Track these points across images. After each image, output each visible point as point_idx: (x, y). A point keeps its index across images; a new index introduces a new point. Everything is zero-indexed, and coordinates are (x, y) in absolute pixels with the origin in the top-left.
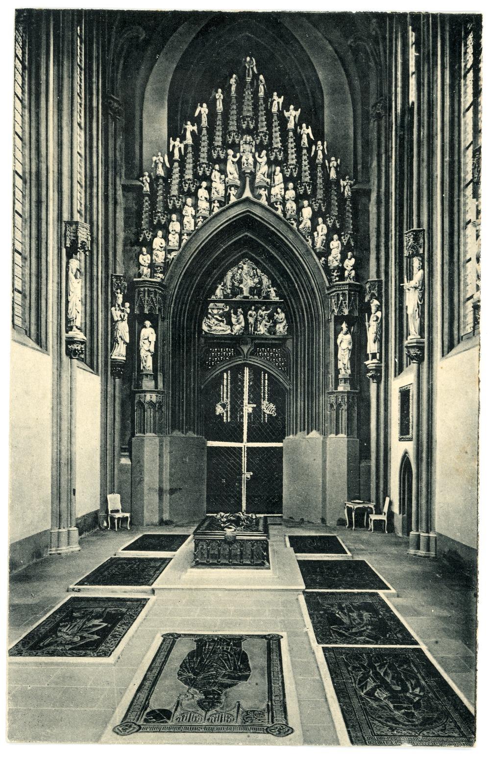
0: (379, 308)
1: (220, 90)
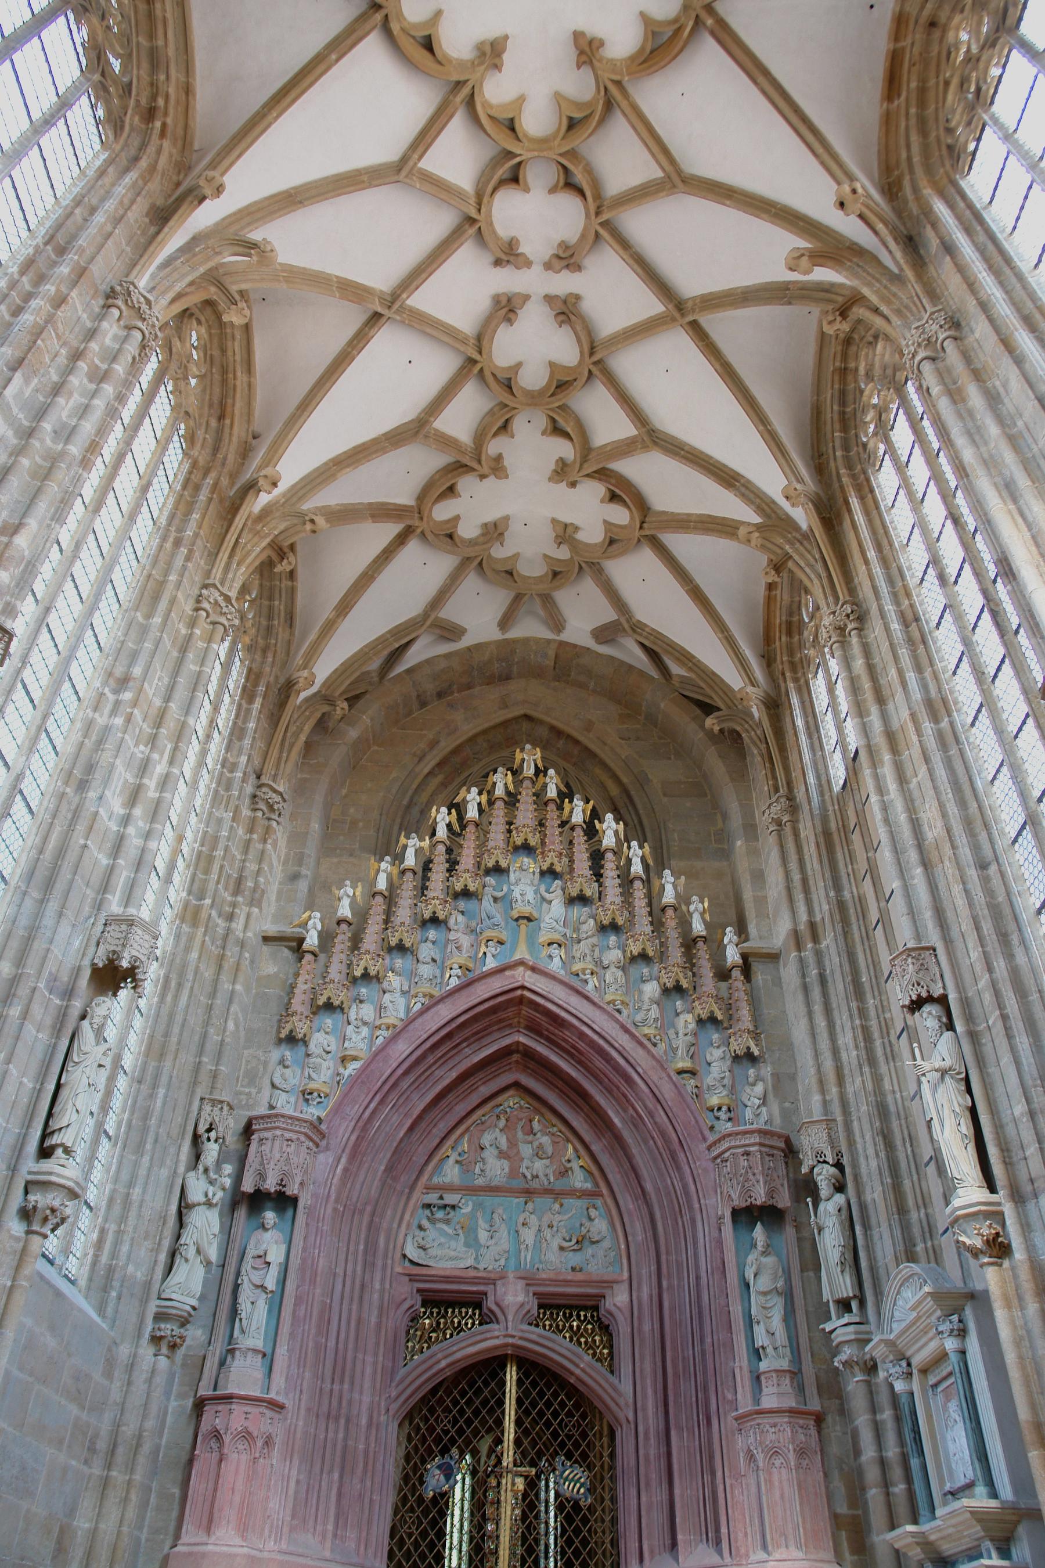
0: (840, 1188)
1: (474, 790)
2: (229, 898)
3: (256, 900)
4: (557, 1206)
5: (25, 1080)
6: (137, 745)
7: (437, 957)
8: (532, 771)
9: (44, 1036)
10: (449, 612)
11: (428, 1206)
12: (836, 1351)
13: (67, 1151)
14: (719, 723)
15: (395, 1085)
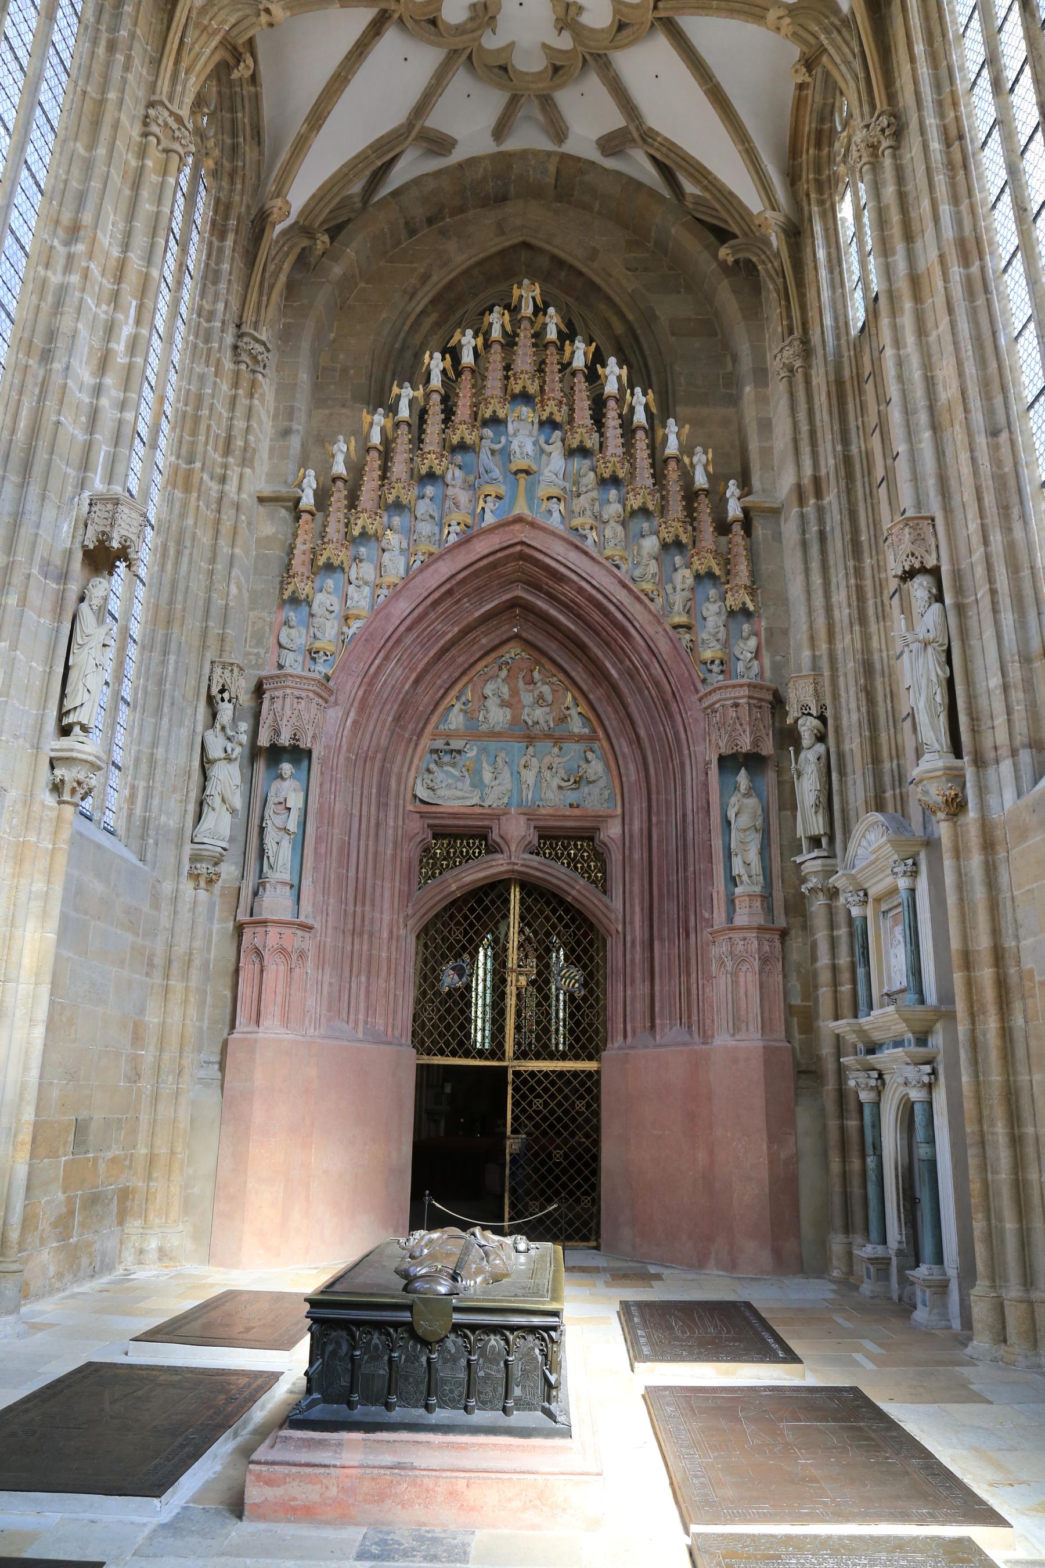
0: (821, 738)
1: (469, 332)
2: (220, 460)
3: (246, 460)
4: (556, 750)
5: (34, 664)
6: (98, 305)
7: (436, 515)
8: (531, 309)
9: (46, 621)
10: (437, 120)
11: (436, 751)
12: (804, 880)
13: (84, 729)
14: (733, 254)
15: (399, 641)
